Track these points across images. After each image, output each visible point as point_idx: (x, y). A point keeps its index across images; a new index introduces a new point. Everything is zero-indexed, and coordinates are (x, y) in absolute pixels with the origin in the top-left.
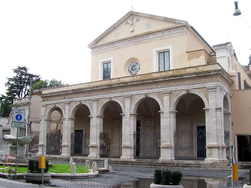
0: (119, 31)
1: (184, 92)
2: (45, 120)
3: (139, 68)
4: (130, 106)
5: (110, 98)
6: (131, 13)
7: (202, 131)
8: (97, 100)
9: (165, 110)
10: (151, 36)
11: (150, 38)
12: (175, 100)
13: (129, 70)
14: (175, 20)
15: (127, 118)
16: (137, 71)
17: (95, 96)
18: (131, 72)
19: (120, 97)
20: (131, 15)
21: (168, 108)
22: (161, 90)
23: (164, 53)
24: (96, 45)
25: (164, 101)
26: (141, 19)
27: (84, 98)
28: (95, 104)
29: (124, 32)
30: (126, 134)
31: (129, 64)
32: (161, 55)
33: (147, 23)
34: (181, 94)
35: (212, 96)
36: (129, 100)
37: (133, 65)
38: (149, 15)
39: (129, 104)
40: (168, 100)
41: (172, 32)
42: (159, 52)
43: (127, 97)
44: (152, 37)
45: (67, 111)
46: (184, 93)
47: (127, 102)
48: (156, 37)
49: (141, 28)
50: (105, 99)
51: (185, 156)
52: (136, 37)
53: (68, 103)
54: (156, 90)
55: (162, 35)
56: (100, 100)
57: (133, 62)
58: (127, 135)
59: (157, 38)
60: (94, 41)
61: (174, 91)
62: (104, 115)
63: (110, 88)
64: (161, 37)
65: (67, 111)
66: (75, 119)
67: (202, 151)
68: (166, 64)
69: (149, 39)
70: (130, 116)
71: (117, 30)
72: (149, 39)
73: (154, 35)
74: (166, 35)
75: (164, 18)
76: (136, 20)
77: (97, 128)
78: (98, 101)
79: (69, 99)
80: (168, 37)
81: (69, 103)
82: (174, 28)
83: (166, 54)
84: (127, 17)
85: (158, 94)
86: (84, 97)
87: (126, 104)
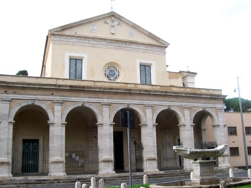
0: (95, 27)
1: (201, 109)
2: (9, 123)
3: (119, 75)
4: (152, 116)
5: (129, 104)
6: (113, 14)
7: (29, 145)
8: (109, 105)
9: (187, 123)
10: (134, 46)
11: (133, 47)
12: (194, 115)
13: (105, 74)
14: (159, 39)
16: (116, 78)
17: (106, 100)
18: (108, 77)
19: (140, 105)
20: (113, 15)
21: (189, 122)
22: (184, 104)
23: (145, 66)
24: (59, 33)
27: (88, 99)
30: (149, 146)
31: (106, 68)
32: (143, 68)
33: (129, 31)
34: (198, 111)
36: (151, 110)
37: (112, 70)
38: (134, 24)
39: (151, 114)
40: (189, 115)
41: (155, 49)
42: (141, 64)
43: (148, 106)
44: (135, 47)
48: (140, 49)
50: (119, 105)
51: (170, 166)
52: (117, 41)
53: (60, 103)
54: (176, 103)
55: (145, 48)
57: (111, 67)
59: (140, 50)
60: (60, 27)
61: (193, 107)
62: (156, 123)
64: (144, 50)
65: (58, 114)
66: (66, 124)
67: (27, 167)
68: (147, 77)
69: (133, 48)
70: (153, 127)
71: (93, 26)
73: (137, 46)
75: (150, 33)
77: (110, 139)
79: (61, 97)
81: (62, 103)
82: (157, 46)
83: (147, 68)
84: (107, 16)
85: (179, 108)
86: (89, 98)
87: (147, 114)
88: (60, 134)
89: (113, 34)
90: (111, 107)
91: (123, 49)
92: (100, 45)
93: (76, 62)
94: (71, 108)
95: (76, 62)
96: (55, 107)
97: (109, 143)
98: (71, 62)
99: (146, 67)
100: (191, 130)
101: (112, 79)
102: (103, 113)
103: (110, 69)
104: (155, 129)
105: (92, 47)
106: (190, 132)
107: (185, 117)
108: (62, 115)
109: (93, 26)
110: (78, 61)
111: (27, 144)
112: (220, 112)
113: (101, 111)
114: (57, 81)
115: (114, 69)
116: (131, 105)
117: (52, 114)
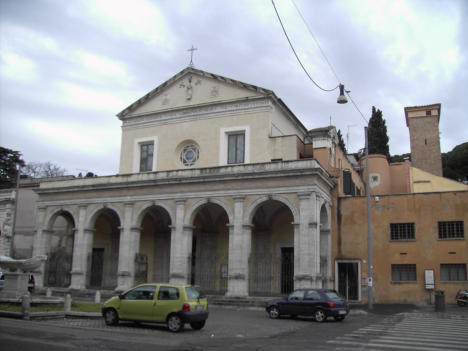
0: (168, 97)
1: (265, 198)
2: (43, 231)
5: (154, 201)
7: (289, 256)
8: (132, 204)
9: (237, 223)
10: (219, 109)
12: (251, 208)
13: (181, 158)
16: (194, 161)
17: (129, 197)
18: (185, 162)
20: (190, 73)
22: (231, 192)
26: (203, 81)
27: (110, 199)
29: (176, 98)
32: (233, 140)
34: (260, 201)
41: (251, 105)
43: (179, 201)
45: (82, 219)
46: (265, 199)
49: (202, 93)
50: (145, 202)
52: (194, 108)
55: (234, 108)
56: (137, 203)
57: (188, 146)
59: (227, 113)
60: (128, 108)
61: (251, 196)
63: (154, 185)
68: (239, 152)
69: (215, 113)
72: (215, 113)
73: (223, 108)
74: (240, 109)
76: (196, 82)
79: (86, 200)
80: (244, 113)
83: (240, 139)
85: (226, 199)
86: (112, 197)
87: (178, 211)
92: (173, 120)
93: (236, 138)
95: (146, 149)
101: (189, 163)
103: (187, 149)
105: (165, 124)
111: (287, 253)
112: (305, 200)
116: (276, 196)
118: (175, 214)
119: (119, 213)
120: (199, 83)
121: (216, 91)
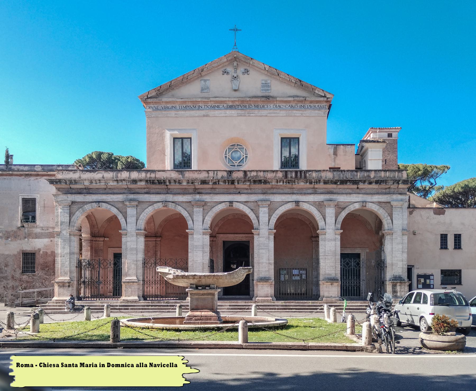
3: (246, 157)
4: (267, 219)
5: (231, 202)
9: (329, 229)
13: (226, 157)
15: (264, 237)
25: (327, 215)
28: (198, 212)
33: (264, 82)
35: (398, 214)
36: (266, 210)
45: (131, 220)
46: (357, 206)
47: (263, 212)
54: (311, 198)
58: (264, 264)
71: (205, 81)
77: (204, 252)
78: (203, 206)
87: (261, 215)
88: (135, 246)
89: (235, 90)
90: (205, 207)
91: (252, 115)
94: (149, 211)
96: (128, 211)
97: (202, 258)
98: (176, 142)
99: (292, 140)
100: (335, 240)
101: (236, 164)
102: (194, 217)
104: (272, 237)
106: (333, 243)
107: (327, 220)
108: (137, 220)
109: (205, 81)
110: (185, 141)
113: (191, 215)
114: (130, 174)
115: (239, 148)
117: (124, 220)
118: (258, 217)
119: (185, 214)
120: (246, 72)
121: (268, 86)
